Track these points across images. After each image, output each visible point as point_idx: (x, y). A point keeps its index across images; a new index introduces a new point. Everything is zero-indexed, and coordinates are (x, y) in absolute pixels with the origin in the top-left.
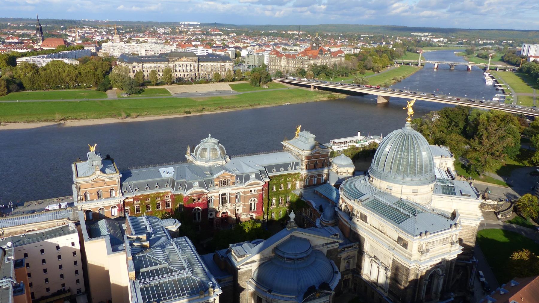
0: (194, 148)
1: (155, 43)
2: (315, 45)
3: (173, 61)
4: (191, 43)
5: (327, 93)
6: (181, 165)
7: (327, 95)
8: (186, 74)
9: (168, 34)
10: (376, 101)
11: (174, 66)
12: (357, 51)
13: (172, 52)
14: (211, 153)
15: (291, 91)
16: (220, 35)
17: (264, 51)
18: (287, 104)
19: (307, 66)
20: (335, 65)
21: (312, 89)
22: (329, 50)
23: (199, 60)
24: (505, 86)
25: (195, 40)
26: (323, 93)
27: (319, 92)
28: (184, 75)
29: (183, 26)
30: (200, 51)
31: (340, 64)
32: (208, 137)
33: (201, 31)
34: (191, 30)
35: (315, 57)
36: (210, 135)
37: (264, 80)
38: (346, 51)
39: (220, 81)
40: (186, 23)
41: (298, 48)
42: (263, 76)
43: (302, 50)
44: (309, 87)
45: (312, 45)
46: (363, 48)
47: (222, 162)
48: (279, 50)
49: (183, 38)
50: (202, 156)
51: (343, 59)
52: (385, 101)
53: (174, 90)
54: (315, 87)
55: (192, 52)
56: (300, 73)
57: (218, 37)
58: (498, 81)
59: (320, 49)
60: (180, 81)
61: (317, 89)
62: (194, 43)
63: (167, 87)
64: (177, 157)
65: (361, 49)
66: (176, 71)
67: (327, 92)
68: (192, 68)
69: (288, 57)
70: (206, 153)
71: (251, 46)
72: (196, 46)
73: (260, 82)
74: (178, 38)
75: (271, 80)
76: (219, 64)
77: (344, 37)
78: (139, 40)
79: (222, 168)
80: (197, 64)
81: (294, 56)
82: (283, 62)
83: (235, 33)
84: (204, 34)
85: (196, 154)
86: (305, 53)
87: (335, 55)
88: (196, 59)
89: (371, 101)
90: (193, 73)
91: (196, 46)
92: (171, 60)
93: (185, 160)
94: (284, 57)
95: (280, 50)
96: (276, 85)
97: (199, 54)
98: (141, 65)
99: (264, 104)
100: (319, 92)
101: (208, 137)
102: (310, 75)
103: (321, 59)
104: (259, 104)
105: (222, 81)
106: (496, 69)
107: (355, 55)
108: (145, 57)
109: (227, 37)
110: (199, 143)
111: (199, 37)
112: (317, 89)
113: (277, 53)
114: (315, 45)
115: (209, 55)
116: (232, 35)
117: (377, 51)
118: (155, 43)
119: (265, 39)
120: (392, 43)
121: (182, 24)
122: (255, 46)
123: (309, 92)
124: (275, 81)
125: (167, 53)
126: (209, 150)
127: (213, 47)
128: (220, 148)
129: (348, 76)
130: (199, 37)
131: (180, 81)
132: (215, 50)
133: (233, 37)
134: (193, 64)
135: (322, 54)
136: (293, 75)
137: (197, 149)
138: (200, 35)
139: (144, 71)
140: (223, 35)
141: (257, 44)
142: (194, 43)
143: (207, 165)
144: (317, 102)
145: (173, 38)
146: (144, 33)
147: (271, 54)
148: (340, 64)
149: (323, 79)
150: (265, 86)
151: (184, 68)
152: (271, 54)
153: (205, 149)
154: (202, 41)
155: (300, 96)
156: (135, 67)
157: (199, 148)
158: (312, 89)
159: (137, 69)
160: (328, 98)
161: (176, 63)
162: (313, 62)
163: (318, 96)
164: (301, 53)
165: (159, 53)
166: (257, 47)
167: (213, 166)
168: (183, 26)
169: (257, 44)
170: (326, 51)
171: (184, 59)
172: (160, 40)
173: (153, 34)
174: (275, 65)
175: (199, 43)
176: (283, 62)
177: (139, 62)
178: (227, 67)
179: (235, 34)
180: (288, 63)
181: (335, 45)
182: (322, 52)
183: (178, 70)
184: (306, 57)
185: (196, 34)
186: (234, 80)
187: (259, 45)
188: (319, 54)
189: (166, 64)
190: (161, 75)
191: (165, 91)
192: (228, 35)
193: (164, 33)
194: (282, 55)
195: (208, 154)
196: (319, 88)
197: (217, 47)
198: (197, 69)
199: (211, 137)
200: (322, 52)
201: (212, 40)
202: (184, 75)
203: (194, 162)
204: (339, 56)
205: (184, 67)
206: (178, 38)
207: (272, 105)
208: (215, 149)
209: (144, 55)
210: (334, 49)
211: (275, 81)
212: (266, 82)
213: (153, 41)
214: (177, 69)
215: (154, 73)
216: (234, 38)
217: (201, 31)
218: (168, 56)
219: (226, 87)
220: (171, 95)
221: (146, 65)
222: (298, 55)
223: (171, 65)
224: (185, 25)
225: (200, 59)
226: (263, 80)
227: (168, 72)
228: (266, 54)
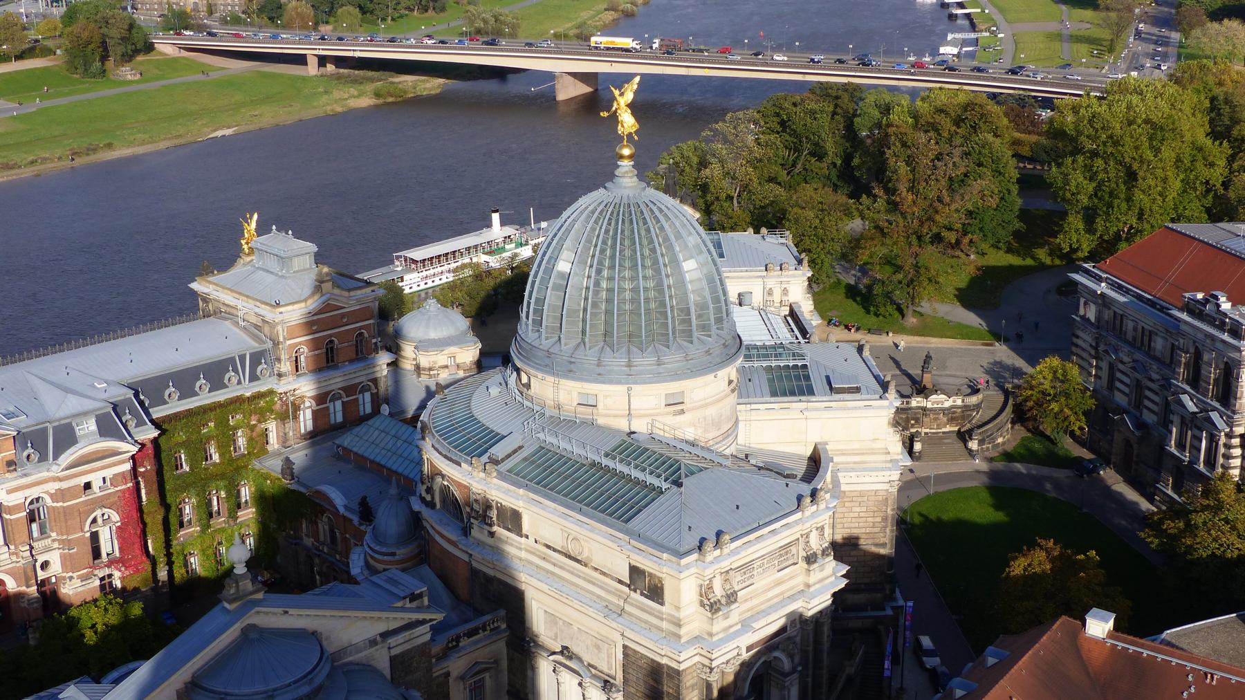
5: (372, 80)
7: (370, 87)
10: (552, 90)
15: (231, 83)
18: (219, 133)
21: (312, 68)
26: (356, 81)
27: (339, 77)
37: (120, 50)
42: (114, 33)
44: (301, 60)
52: (584, 89)
54: (323, 61)
56: (261, 10)
61: (330, 68)
67: (370, 74)
73: (104, 58)
75: (149, 48)
89: (535, 97)
96: (171, 63)
99: (131, 144)
100: (339, 77)
102: (301, 16)
104: (109, 146)
112: (330, 68)
123: (305, 79)
124: (166, 47)
129: (443, 9)
136: (236, 21)
144: (336, 115)
149: (351, 28)
150: (127, 73)
155: (268, 99)
158: (312, 68)
160: (377, 95)
163: (336, 94)
196: (340, 62)
207: (162, 145)
212: (128, 58)
226: (116, 51)
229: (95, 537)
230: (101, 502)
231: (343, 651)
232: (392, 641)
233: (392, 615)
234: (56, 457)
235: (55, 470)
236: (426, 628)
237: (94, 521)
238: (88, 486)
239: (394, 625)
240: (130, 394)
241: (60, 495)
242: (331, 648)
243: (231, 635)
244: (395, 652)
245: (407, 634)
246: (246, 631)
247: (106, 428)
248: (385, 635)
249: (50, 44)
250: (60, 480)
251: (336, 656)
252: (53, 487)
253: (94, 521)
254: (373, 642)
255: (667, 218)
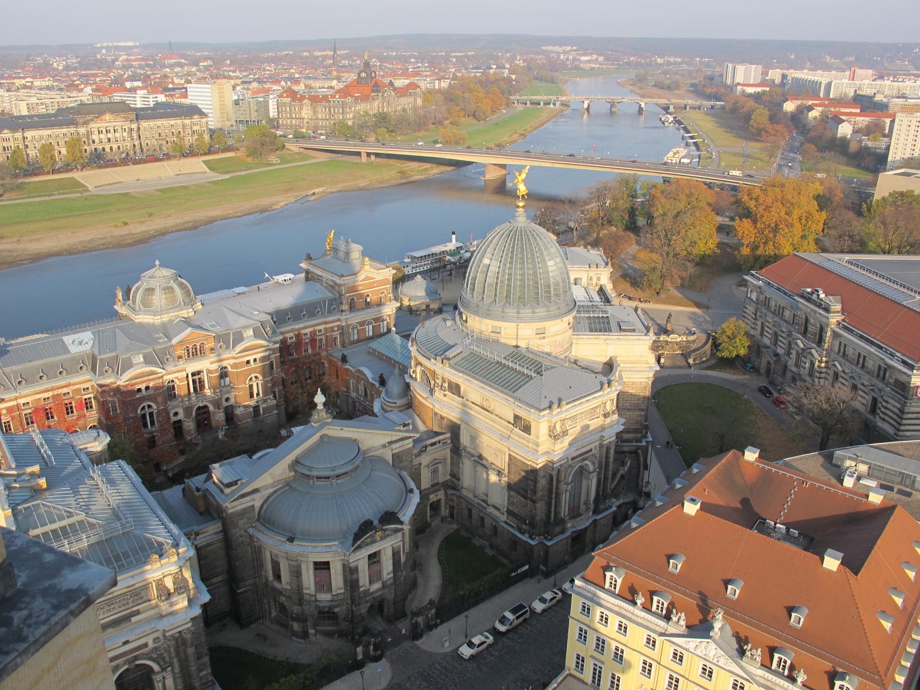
0: (129, 290)
1: (48, 88)
2: (363, 75)
3: (86, 123)
4: (122, 84)
6: (106, 327)
8: (115, 147)
9: (75, 69)
11: (89, 133)
12: (444, 84)
13: (82, 104)
14: (164, 296)
16: (181, 65)
17: (267, 91)
19: (351, 116)
20: (404, 110)
21: (364, 159)
22: (391, 83)
23: (138, 118)
24: (699, 136)
25: (132, 79)
28: (111, 149)
29: (104, 51)
30: (140, 99)
31: (415, 109)
32: (155, 266)
33: (143, 59)
34: (121, 59)
35: (365, 98)
36: (157, 263)
38: (424, 84)
39: (184, 155)
40: (110, 44)
41: (334, 83)
43: (341, 86)
44: (359, 154)
45: (359, 75)
46: (455, 78)
47: (188, 313)
48: (296, 88)
49: (107, 75)
50: (146, 303)
51: (419, 102)
53: (93, 180)
54: (369, 155)
55: (123, 102)
57: (177, 69)
58: (689, 128)
59: (373, 82)
60: (99, 160)
62: (128, 85)
63: (77, 175)
64: (96, 311)
65: (453, 79)
66: (94, 142)
68: (125, 134)
69: (315, 100)
70: (154, 297)
71: (243, 83)
72: (133, 90)
74: (96, 75)
76: (179, 122)
77: (421, 58)
78: (14, 83)
79: (187, 322)
80: (134, 126)
81: (325, 98)
82: (306, 112)
83: (211, 59)
84: (148, 65)
85: (134, 302)
86: (345, 92)
87: (403, 92)
88: (133, 116)
90: (129, 145)
91: (133, 90)
92: (82, 120)
93: (116, 315)
94: (306, 101)
95: (300, 88)
97: (139, 106)
98: (19, 135)
101: (155, 266)
103: (377, 102)
105: (192, 153)
106: (685, 108)
107: (440, 91)
108: (30, 117)
109: (194, 69)
110: (138, 279)
111: (139, 71)
112: (373, 157)
113: (292, 94)
114: (363, 75)
115: (158, 105)
116: (206, 64)
117: (481, 82)
118: (48, 88)
119: (270, 68)
120: (508, 66)
121: (102, 48)
122: (250, 82)
124: (293, 147)
125: (72, 108)
126: (158, 291)
127: (166, 90)
128: (181, 285)
130: (139, 71)
131: (99, 160)
132: (172, 96)
133: (207, 68)
134: (127, 125)
135: (378, 91)
137: (136, 292)
138: (141, 67)
139: (27, 147)
140: (186, 65)
141: (254, 80)
142: (128, 85)
143: (157, 320)
145: (86, 76)
146: (23, 68)
147: (281, 96)
148: (415, 109)
151: (109, 135)
152: (281, 96)
153: (150, 291)
154: (146, 79)
156: (8, 140)
157: (138, 289)
158: (364, 159)
159: (11, 144)
161: (92, 125)
162: (362, 107)
164: (338, 91)
165: (56, 107)
166: (255, 85)
167: (171, 321)
168: (104, 51)
169: (254, 80)
170: (386, 86)
171: (107, 117)
172: (58, 80)
173: (43, 70)
174: (291, 118)
175: (139, 84)
176: (306, 112)
177: (14, 130)
178: (195, 128)
179: (210, 62)
180: (315, 112)
181: (405, 74)
182: (377, 87)
183: (97, 141)
184: (349, 100)
185: (131, 66)
186: (209, 152)
187: (260, 81)
188: (373, 91)
189: (72, 129)
190: (64, 151)
191: (76, 184)
192: (197, 65)
193: (67, 68)
194: (303, 98)
195: (159, 299)
196: (378, 155)
197: (174, 89)
198: (135, 135)
199: (160, 266)
200: (377, 87)
201: (166, 76)
202: (111, 149)
203: (132, 316)
204: (411, 94)
205: (109, 133)
206: (96, 75)
208: (169, 289)
209: (25, 112)
210: (400, 83)
211: (293, 147)
213: (44, 84)
214: (95, 137)
215: (47, 149)
216: (208, 70)
217: (143, 59)
218: (73, 113)
219: (196, 166)
220: (88, 190)
221: (29, 134)
222: (333, 96)
223: (82, 130)
224: (107, 48)
225: (140, 115)
227: (74, 144)
228: (271, 97)
229: (251, 387)
230: (252, 371)
231: (369, 450)
232: (394, 446)
233: (393, 433)
234: (233, 347)
235: (233, 354)
236: (411, 440)
237: (251, 379)
238: (248, 362)
239: (394, 438)
240: (269, 317)
241: (235, 366)
242: (363, 448)
243: (315, 438)
244: (394, 452)
245: (400, 443)
246: (321, 437)
247: (257, 335)
248: (390, 443)
249: (237, 145)
250: (235, 358)
251: (365, 452)
252: (232, 362)
253: (251, 379)
254: (384, 446)
255: (541, 239)
